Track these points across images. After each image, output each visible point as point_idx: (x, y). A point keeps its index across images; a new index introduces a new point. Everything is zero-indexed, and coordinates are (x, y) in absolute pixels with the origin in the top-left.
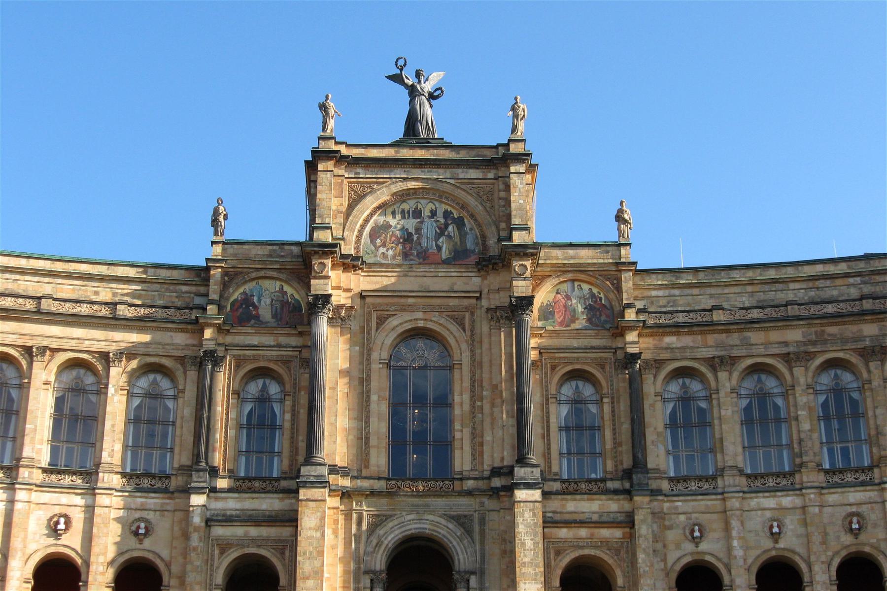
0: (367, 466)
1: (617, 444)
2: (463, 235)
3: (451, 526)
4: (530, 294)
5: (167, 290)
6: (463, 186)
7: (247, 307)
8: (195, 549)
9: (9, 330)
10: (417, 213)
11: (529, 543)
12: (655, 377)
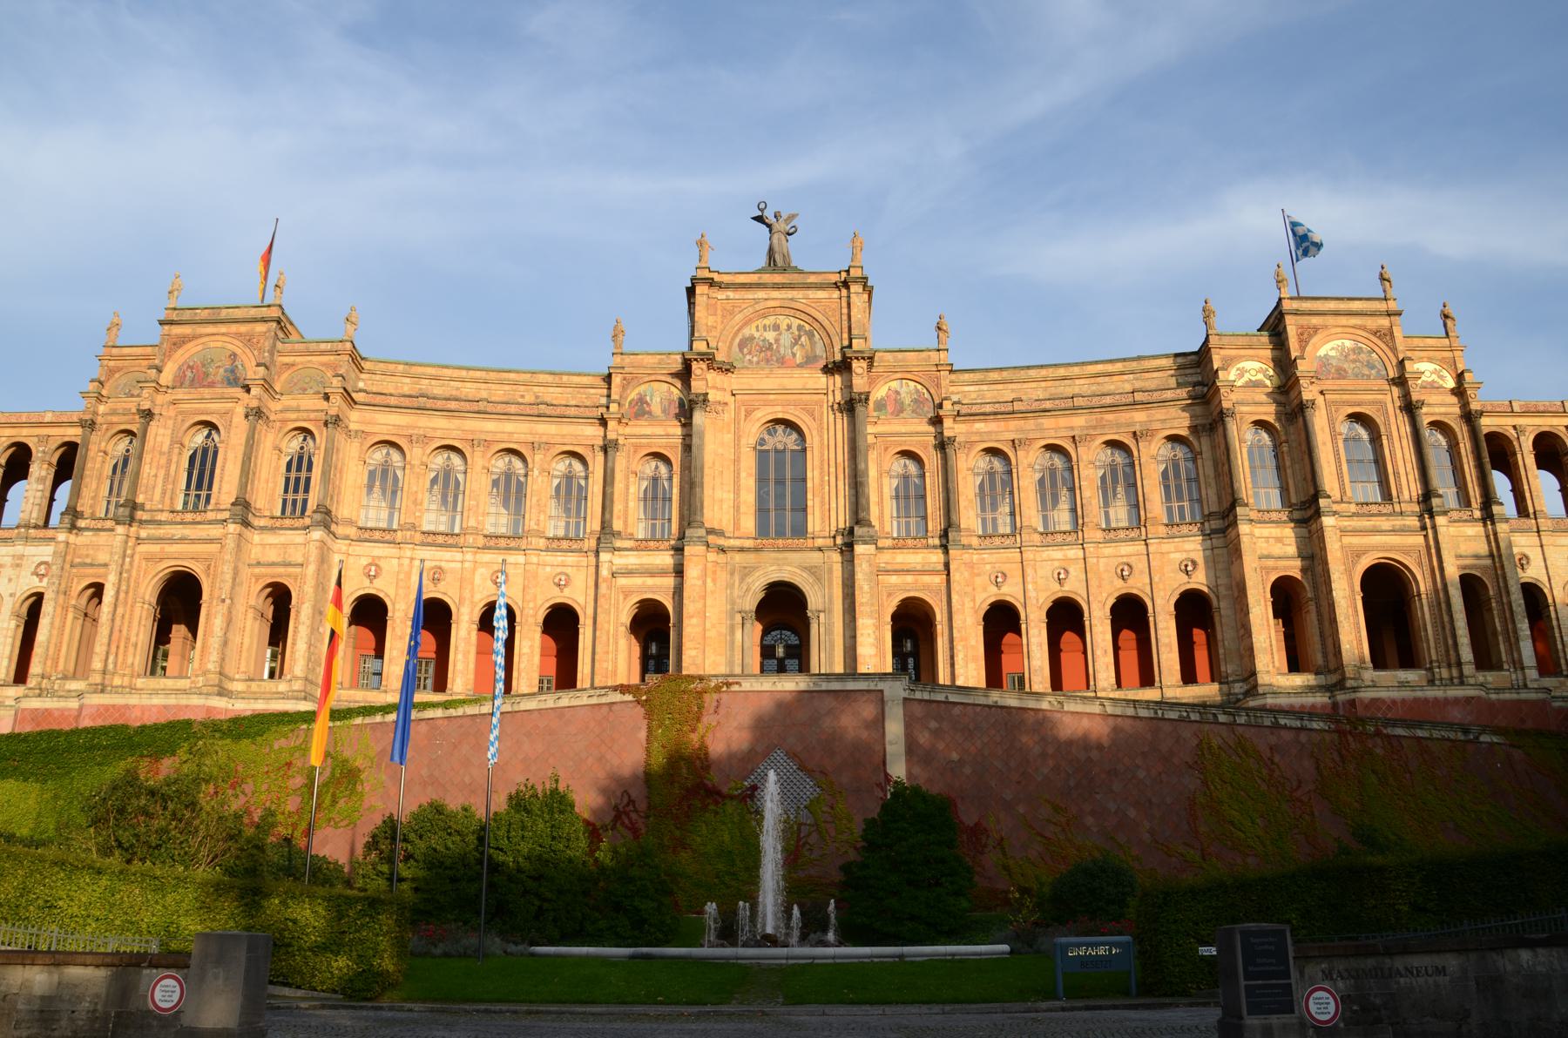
0: (738, 529)
2: (813, 344)
3: (805, 575)
4: (867, 390)
5: (579, 392)
6: (813, 305)
7: (642, 404)
8: (604, 596)
9: (453, 427)
10: (776, 327)
11: (866, 588)
12: (967, 455)
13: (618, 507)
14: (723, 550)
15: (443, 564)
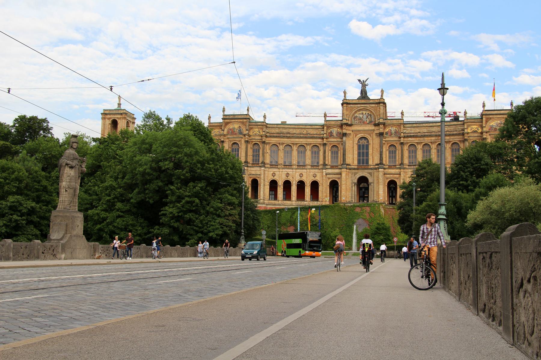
1: (399, 159)
10: (363, 114)
11: (381, 179)
13: (327, 158)
14: (350, 169)
15: (289, 172)
